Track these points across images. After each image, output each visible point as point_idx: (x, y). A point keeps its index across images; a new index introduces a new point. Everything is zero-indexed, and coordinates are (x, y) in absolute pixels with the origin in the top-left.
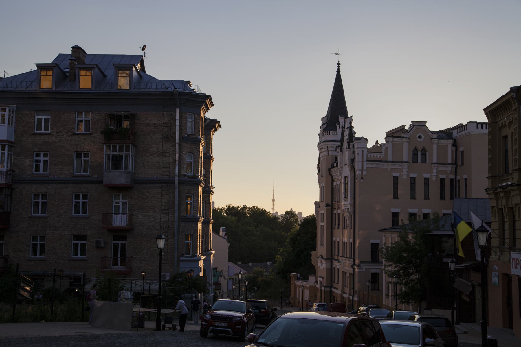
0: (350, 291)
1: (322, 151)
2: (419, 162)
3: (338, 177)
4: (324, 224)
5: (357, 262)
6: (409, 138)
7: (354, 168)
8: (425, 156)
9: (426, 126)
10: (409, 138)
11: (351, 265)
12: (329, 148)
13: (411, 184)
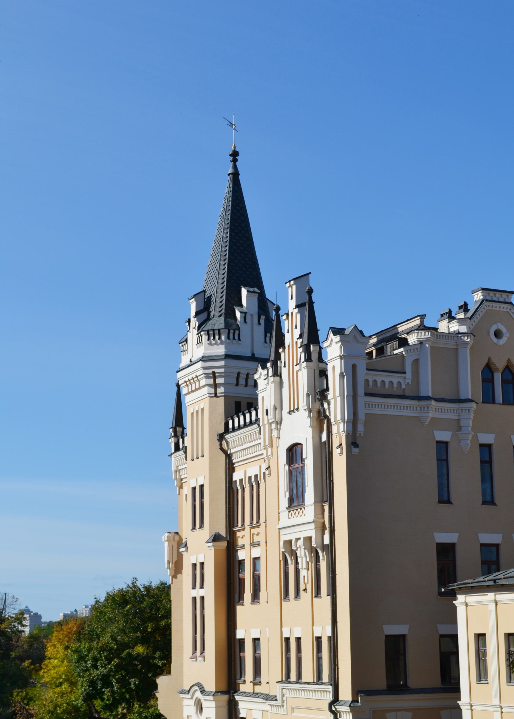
2: (497, 401)
9: (511, 303)
11: (329, 701)
12: (220, 377)
13: (482, 462)
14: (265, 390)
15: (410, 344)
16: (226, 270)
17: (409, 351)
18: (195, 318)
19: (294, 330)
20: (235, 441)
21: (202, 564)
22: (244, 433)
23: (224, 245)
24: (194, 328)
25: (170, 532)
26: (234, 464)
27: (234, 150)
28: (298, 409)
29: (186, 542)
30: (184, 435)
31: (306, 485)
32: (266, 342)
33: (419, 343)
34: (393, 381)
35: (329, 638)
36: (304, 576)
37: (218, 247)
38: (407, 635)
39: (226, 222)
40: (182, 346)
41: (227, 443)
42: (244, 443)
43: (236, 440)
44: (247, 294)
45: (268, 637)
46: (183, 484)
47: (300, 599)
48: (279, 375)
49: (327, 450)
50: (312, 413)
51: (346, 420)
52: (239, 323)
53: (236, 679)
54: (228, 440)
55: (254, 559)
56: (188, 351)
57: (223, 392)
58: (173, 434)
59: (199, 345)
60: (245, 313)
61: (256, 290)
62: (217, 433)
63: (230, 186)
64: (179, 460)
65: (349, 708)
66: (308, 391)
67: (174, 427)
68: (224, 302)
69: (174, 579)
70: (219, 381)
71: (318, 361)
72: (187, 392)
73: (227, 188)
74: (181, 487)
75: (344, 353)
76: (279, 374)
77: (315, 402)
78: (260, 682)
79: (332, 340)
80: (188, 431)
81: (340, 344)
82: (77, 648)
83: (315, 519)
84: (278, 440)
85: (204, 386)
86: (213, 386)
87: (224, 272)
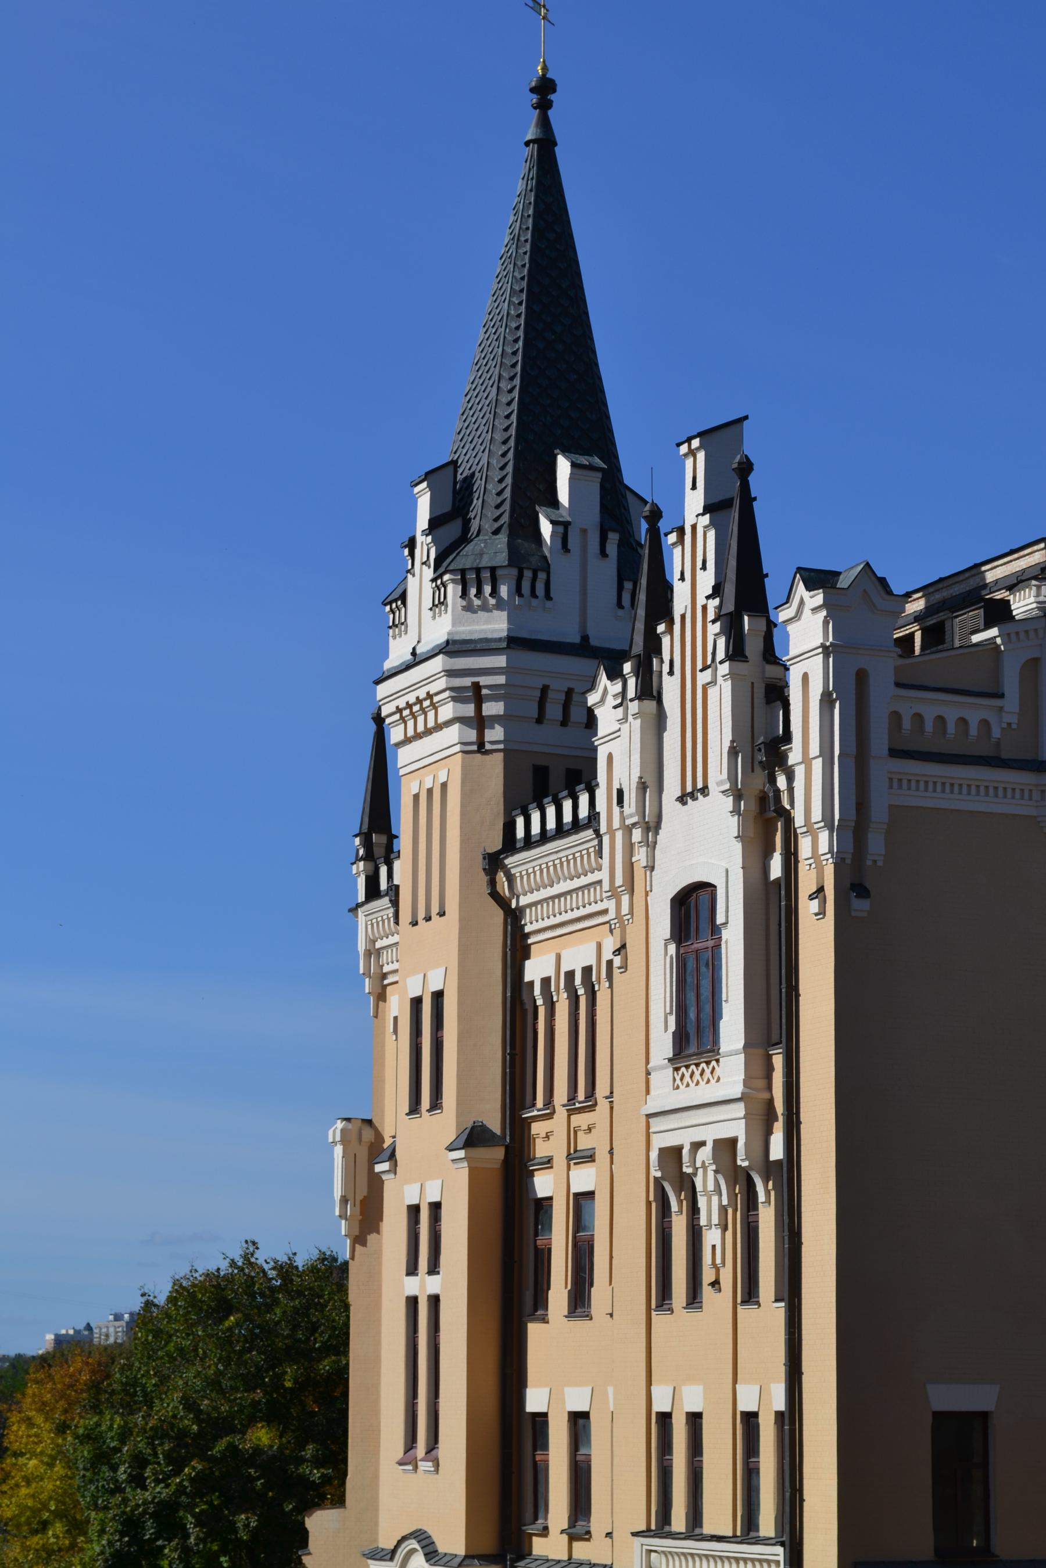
3: (600, 907)
7: (788, 819)
14: (615, 735)
15: (1017, 618)
16: (515, 405)
17: (1013, 637)
18: (427, 535)
19: (699, 573)
20: (532, 875)
21: (436, 1208)
22: (557, 852)
23: (510, 338)
24: (424, 563)
25: (348, 1120)
26: (527, 936)
27: (544, 75)
28: (704, 791)
29: (392, 1147)
30: (392, 856)
31: (724, 997)
32: (620, 605)
33: (1041, 614)
34: (967, 718)
35: (779, 1415)
36: (714, 1247)
37: (494, 342)
38: (992, 1412)
39: (516, 274)
40: (392, 611)
41: (510, 879)
42: (555, 880)
43: (534, 872)
44: (571, 474)
45: (612, 1410)
46: (388, 988)
47: (701, 1307)
48: (654, 697)
49: (783, 903)
50: (742, 803)
51: (836, 823)
52: (547, 553)
53: (521, 1523)
54: (513, 871)
55: (577, 1195)
56: (407, 627)
57: (502, 738)
58: (361, 852)
59: (437, 610)
60: (566, 525)
61: (597, 461)
62: (482, 850)
63: (531, 176)
64: (378, 923)
66: (732, 742)
67: (365, 833)
68: (507, 493)
69: (357, 1245)
70: (493, 708)
71: (761, 658)
72: (401, 737)
73: (521, 180)
74: (381, 996)
75: (833, 639)
76: (655, 693)
77: (753, 771)
78: (588, 1532)
79: (802, 602)
80: (404, 844)
81: (824, 613)
82: (91, 1429)
83: (747, 1090)
84: (648, 873)
85: (448, 723)
86: (475, 724)
87: (510, 411)
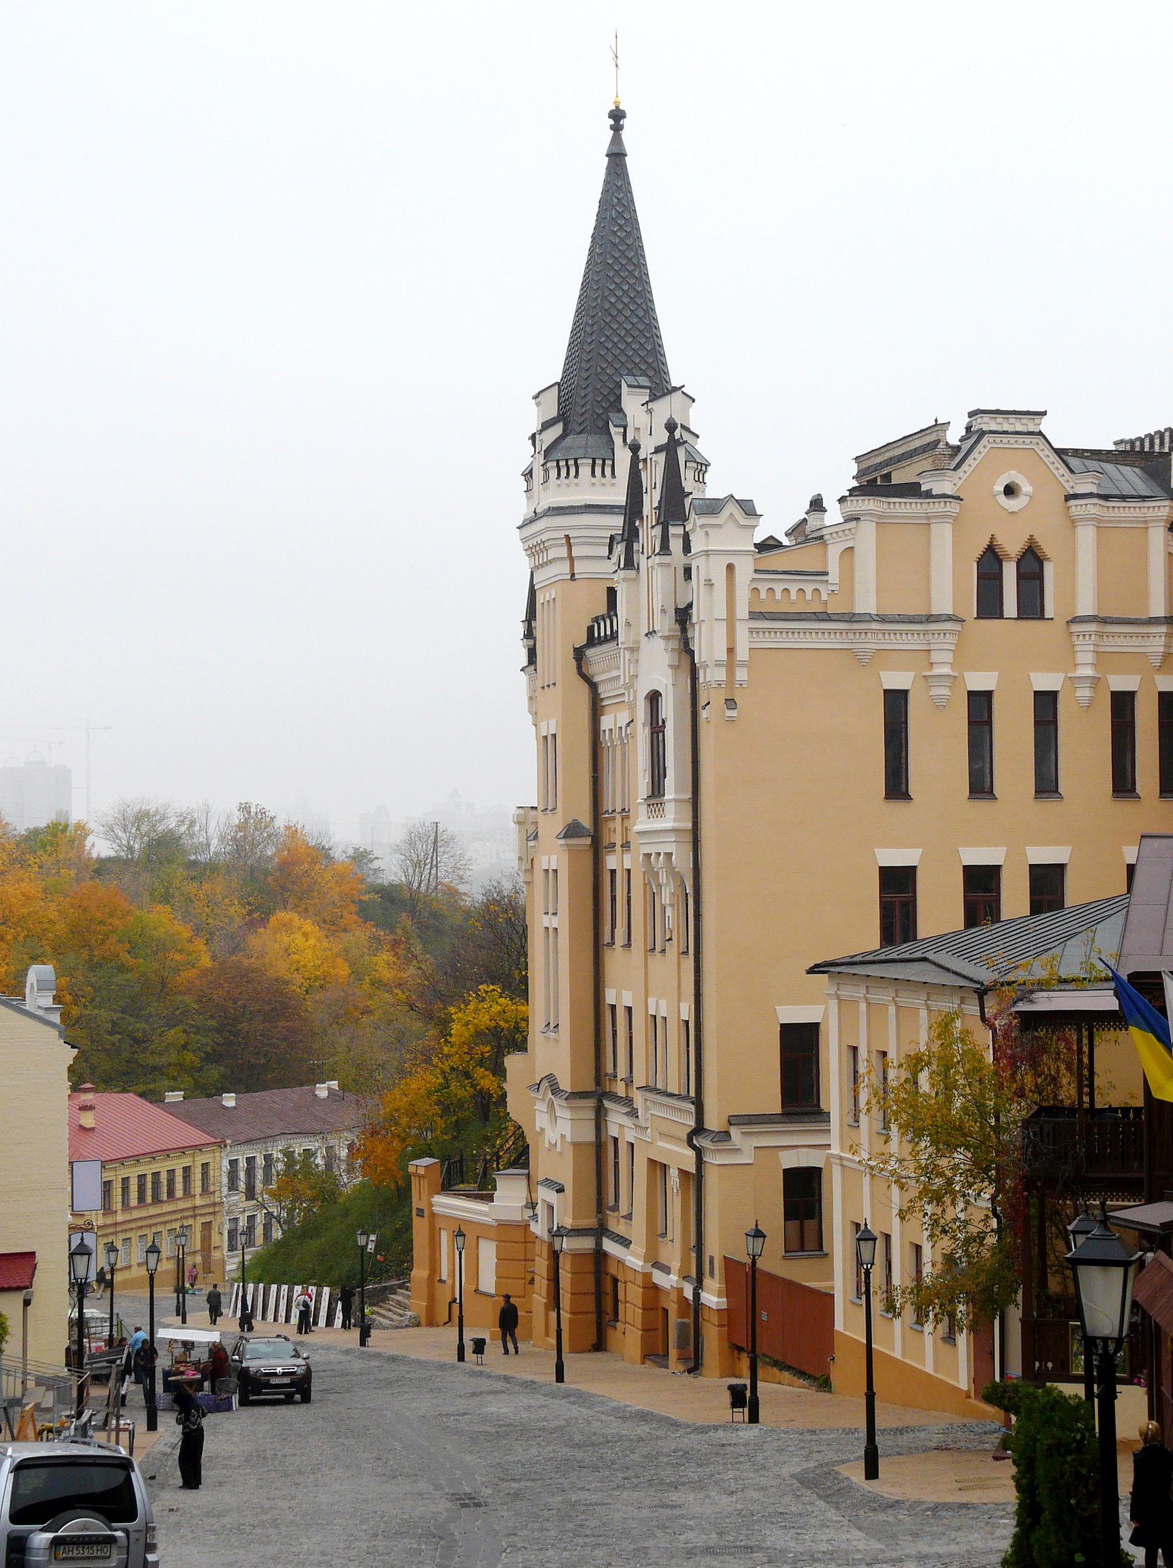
0: (685, 1260)
1: (543, 558)
4: (560, 922)
5: (713, 1122)
6: (958, 498)
8: (1038, 582)
9: (1040, 433)
10: (958, 498)
27: (617, 107)
65: (711, 1143)
